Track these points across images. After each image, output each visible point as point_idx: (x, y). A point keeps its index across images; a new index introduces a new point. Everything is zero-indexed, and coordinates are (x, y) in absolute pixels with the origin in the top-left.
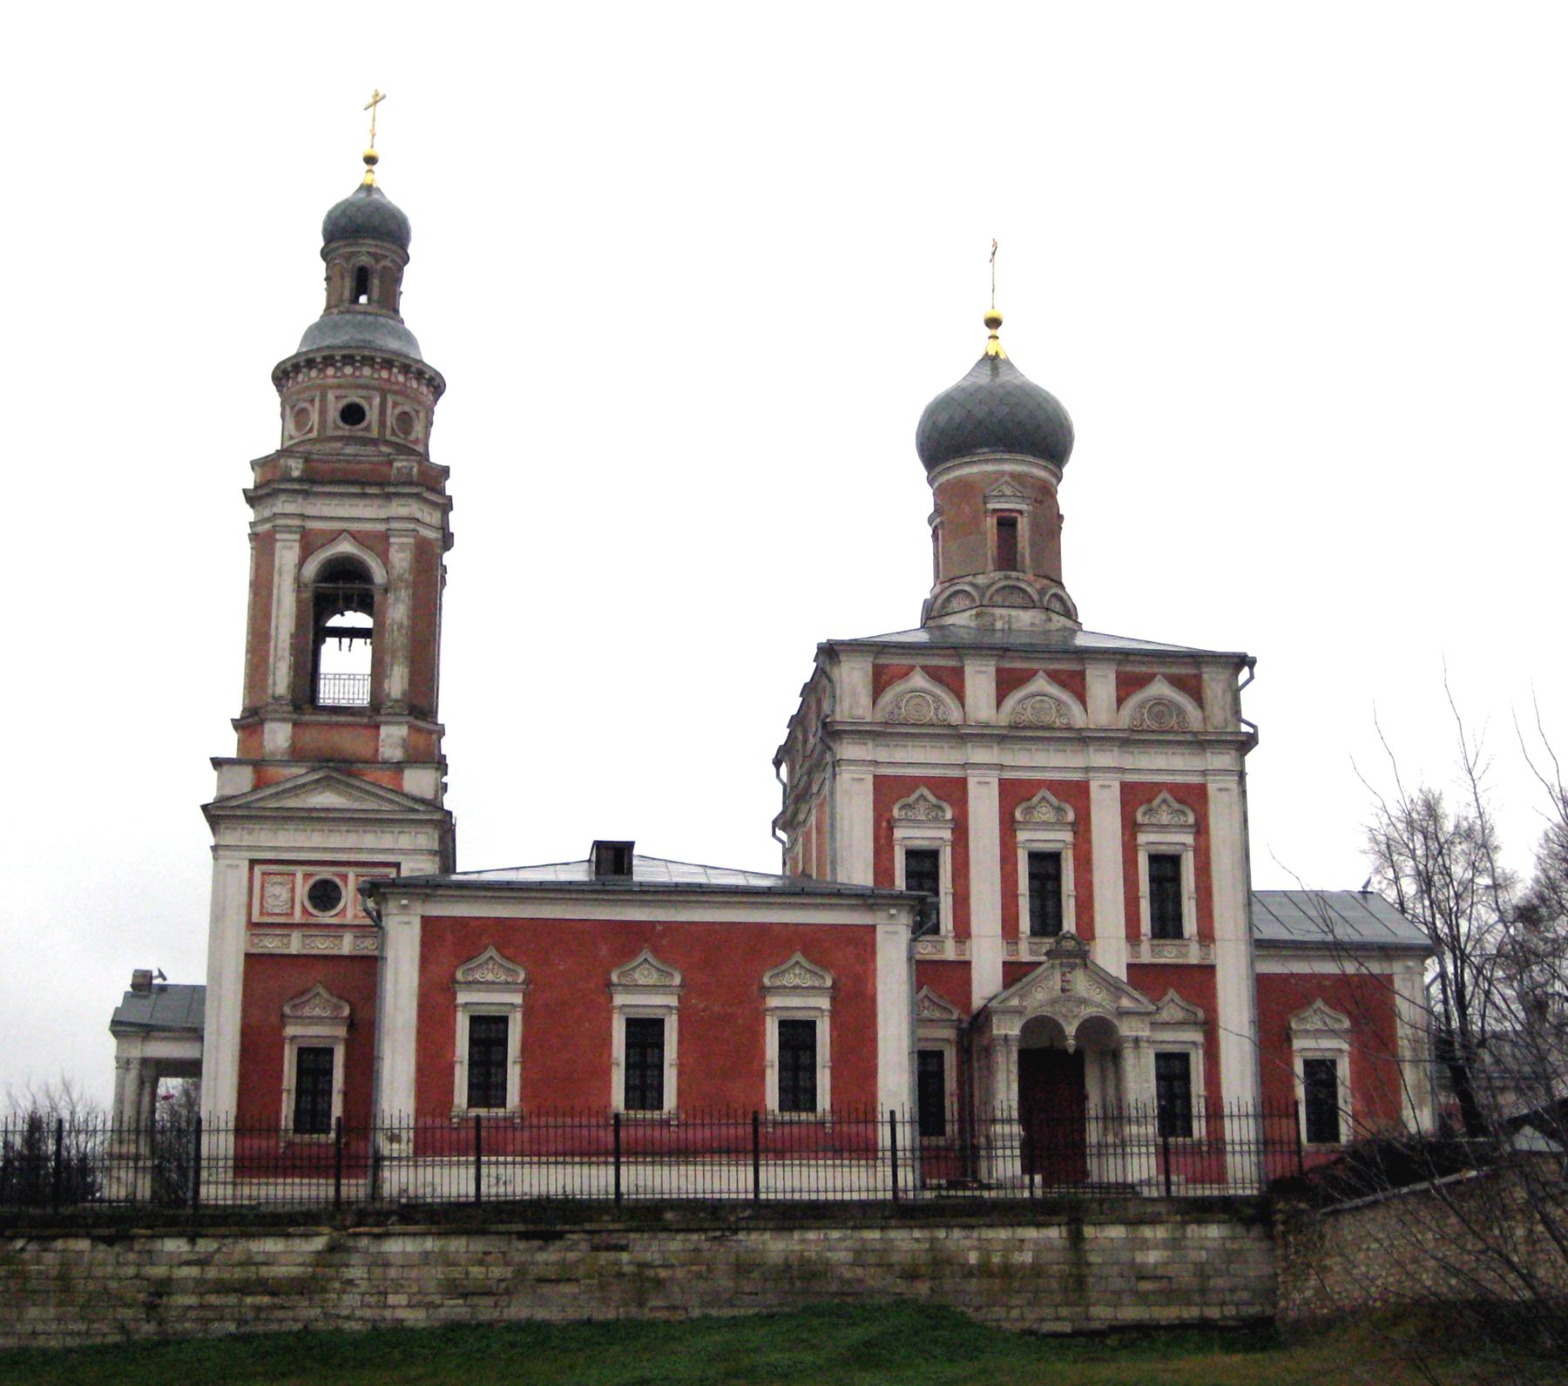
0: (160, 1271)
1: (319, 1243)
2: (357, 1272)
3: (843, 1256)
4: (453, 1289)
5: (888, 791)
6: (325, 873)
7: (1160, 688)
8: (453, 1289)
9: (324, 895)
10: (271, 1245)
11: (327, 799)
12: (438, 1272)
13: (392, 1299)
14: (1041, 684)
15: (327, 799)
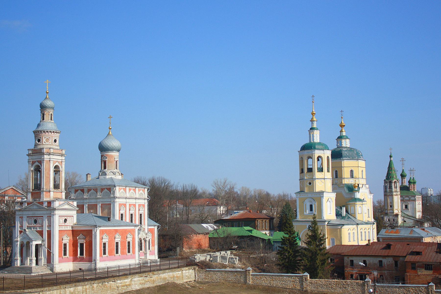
0: (118, 285)
1: (130, 280)
2: (133, 283)
3: (167, 276)
4: (140, 284)
5: (120, 205)
6: (66, 218)
7: (141, 192)
8: (140, 284)
9: (65, 221)
10: (126, 280)
11: (66, 207)
12: (139, 282)
13: (136, 286)
14: (132, 191)
15: (66, 207)
